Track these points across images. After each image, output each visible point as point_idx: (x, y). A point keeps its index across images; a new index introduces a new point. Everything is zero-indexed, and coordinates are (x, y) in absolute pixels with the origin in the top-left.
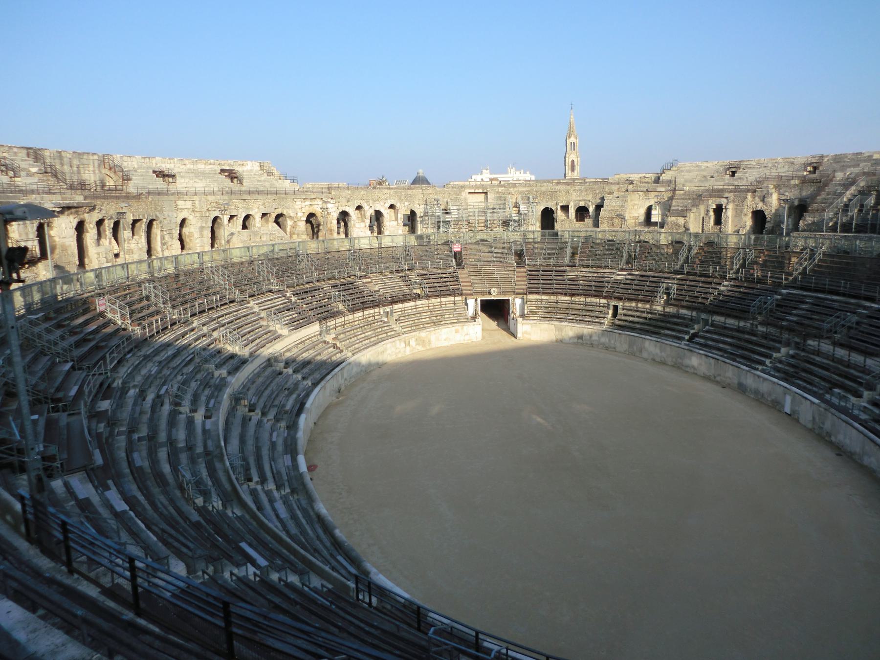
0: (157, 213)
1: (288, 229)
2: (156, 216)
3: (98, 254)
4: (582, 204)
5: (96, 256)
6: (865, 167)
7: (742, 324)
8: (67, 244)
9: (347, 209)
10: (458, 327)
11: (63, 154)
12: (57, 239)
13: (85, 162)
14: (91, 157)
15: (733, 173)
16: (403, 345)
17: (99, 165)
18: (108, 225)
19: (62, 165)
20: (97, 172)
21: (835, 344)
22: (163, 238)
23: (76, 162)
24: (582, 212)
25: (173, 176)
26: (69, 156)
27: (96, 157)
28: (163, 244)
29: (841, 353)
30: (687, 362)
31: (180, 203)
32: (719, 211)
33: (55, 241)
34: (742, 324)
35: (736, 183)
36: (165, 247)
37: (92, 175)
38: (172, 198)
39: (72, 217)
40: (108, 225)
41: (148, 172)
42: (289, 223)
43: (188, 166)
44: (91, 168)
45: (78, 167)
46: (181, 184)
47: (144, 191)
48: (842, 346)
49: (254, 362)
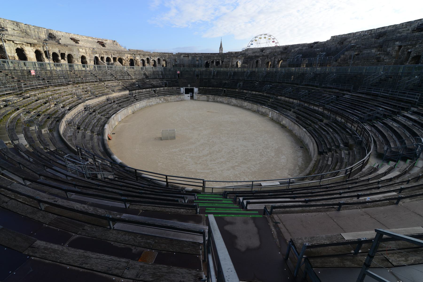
1: (123, 63)
4: (218, 60)
6: (300, 47)
7: (260, 93)
9: (143, 59)
10: (177, 96)
13: (41, 31)
15: (262, 51)
16: (159, 100)
19: (30, 30)
21: (285, 97)
24: (218, 63)
27: (45, 30)
29: (287, 99)
30: (244, 105)
32: (257, 62)
34: (260, 93)
35: (263, 54)
42: (124, 61)
43: (85, 38)
44: (44, 33)
46: (81, 43)
48: (287, 97)
49: (99, 98)
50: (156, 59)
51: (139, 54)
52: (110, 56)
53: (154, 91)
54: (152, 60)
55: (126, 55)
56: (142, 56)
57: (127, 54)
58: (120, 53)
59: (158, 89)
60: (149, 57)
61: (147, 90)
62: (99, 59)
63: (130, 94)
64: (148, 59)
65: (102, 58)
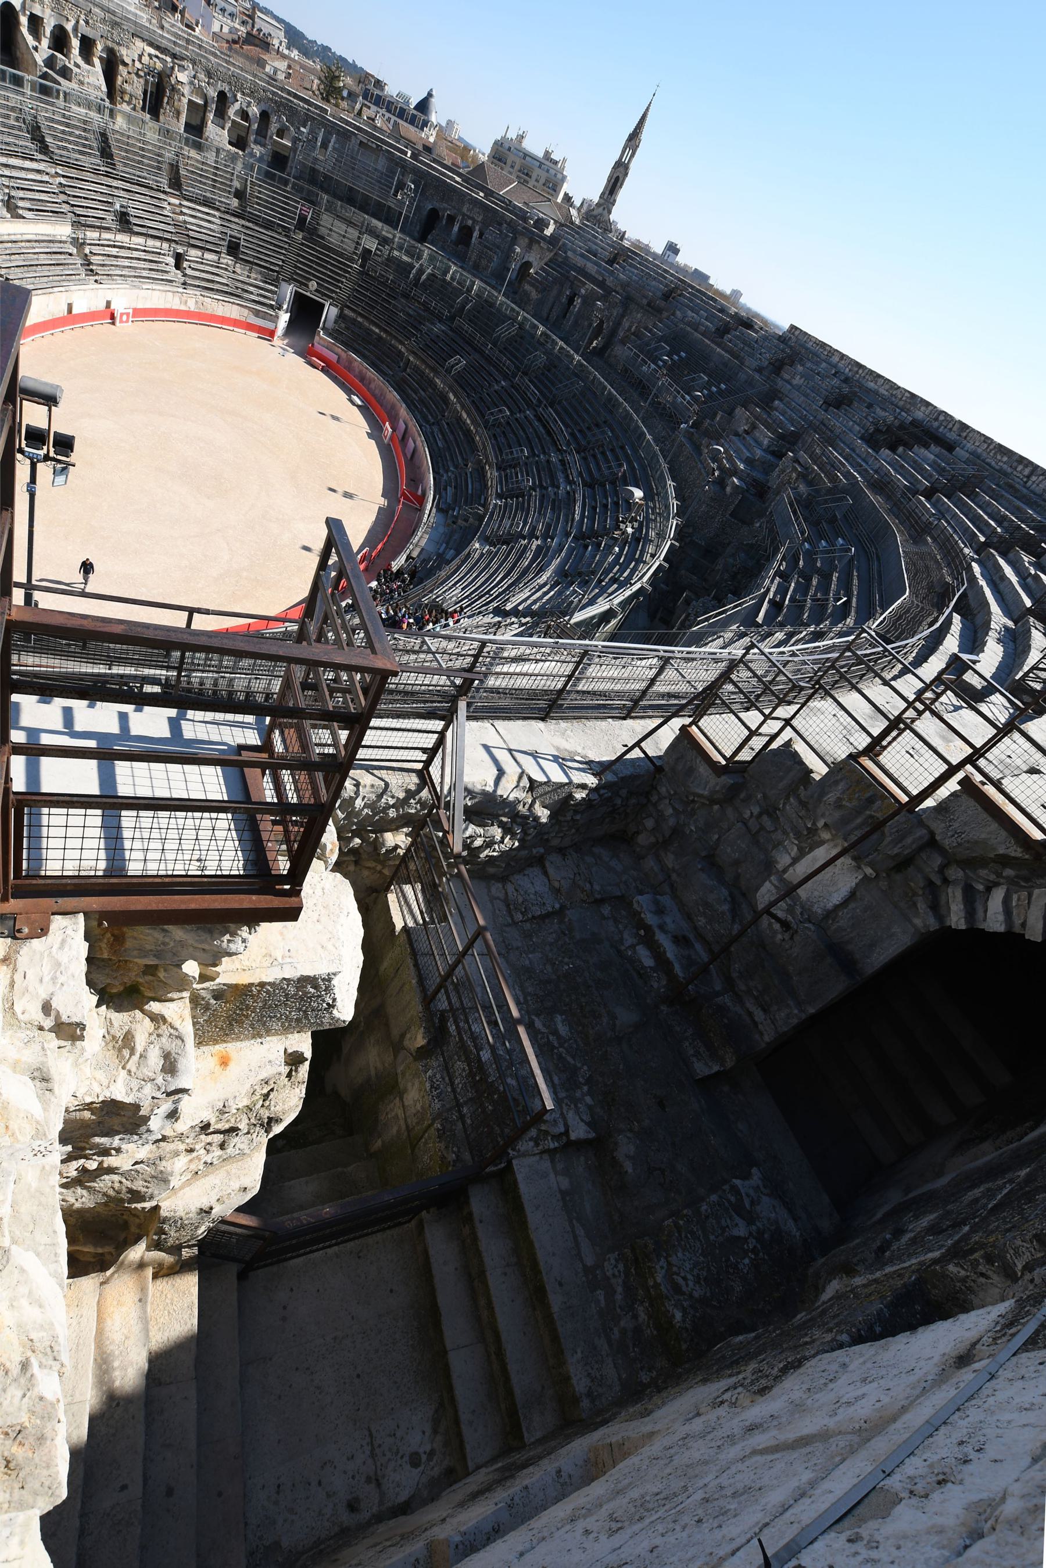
50: (254, 110)
51: (194, 63)
52: (69, 27)
53: (179, 259)
54: (237, 106)
55: (140, 44)
56: (202, 76)
57: (144, 40)
58: (115, 24)
59: (194, 253)
60: (226, 88)
61: (151, 242)
62: (24, 20)
63: (76, 242)
64: (222, 95)
65: (35, 22)
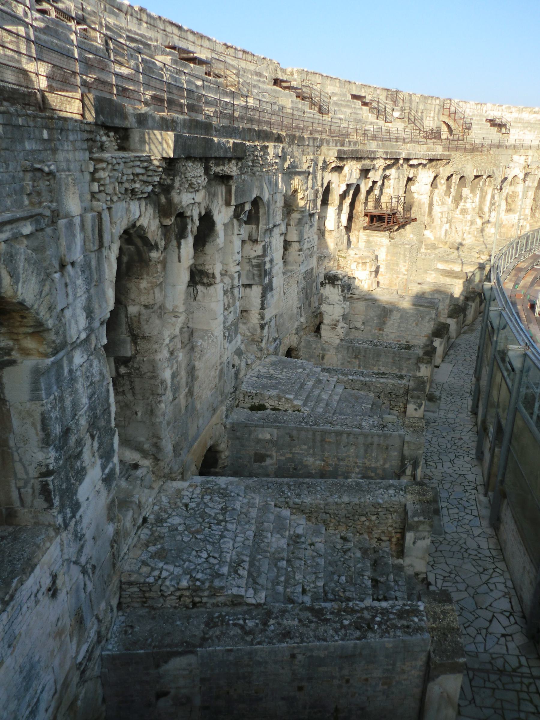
0: (495, 169)
2: (493, 173)
3: (442, 213)
5: (440, 215)
8: (422, 201)
11: (413, 97)
12: (415, 195)
14: (434, 102)
17: (439, 111)
18: (455, 179)
20: (436, 118)
22: (493, 197)
23: (421, 107)
25: (504, 126)
26: (417, 100)
27: (438, 102)
28: (492, 204)
31: (516, 158)
33: (413, 198)
36: (493, 208)
37: (431, 122)
38: (510, 151)
39: (431, 170)
40: (455, 179)
41: (482, 120)
45: (422, 113)
47: (486, 142)
